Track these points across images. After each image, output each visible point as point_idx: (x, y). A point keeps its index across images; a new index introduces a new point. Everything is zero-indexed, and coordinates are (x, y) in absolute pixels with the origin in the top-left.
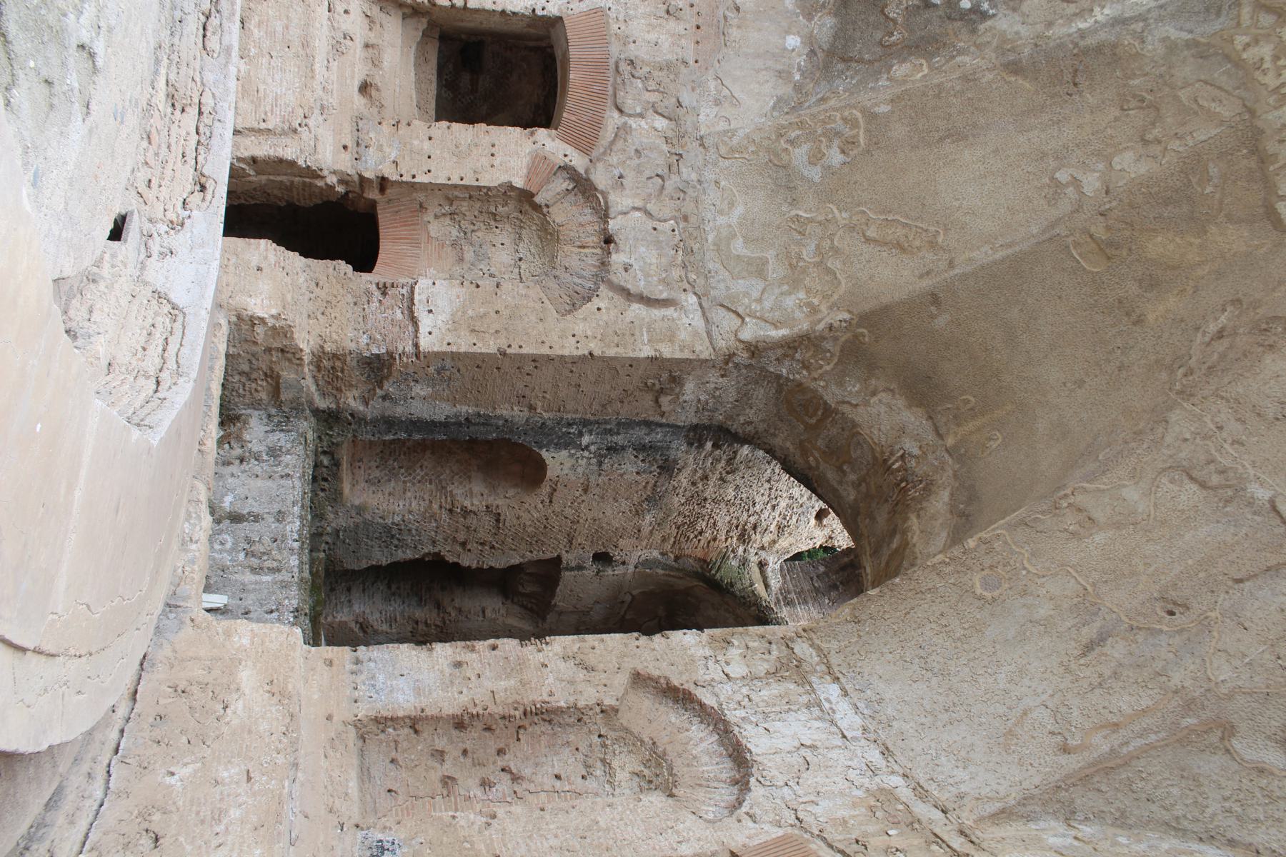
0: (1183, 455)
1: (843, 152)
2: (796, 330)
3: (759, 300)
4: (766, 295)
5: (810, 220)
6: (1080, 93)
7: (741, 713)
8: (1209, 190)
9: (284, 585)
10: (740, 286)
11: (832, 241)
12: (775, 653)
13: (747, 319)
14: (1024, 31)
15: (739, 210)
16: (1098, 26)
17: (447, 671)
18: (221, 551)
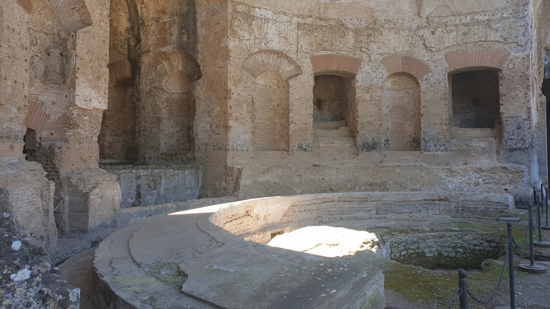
7: (263, 45)
9: (165, 174)
12: (241, 19)
17: (238, 123)
18: (152, 200)
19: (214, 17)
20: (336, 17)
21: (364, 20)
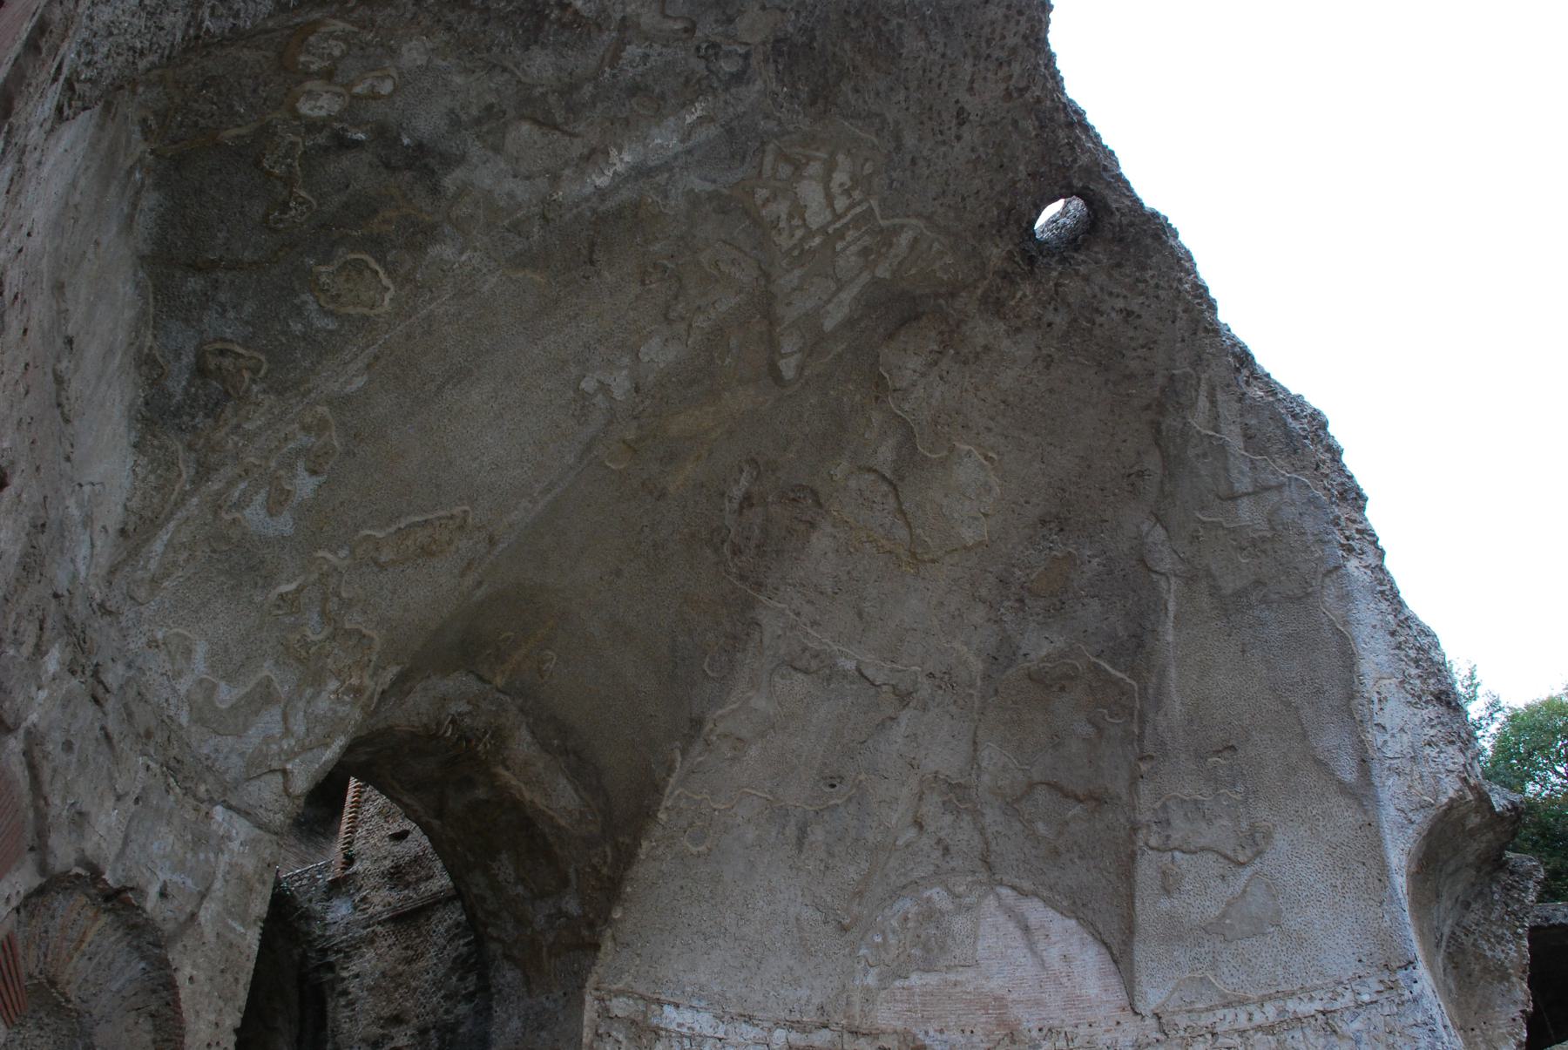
0: (782, 652)
1: (313, 472)
2: (351, 729)
3: (287, 732)
4: (292, 720)
5: (299, 590)
6: (598, 274)
8: (728, 360)
10: (254, 736)
11: (339, 595)
12: (621, 1037)
13: (289, 766)
14: (521, 190)
15: (201, 649)
16: (620, 181)
19: (544, 1034)
20: (899, 1025)
21: (978, 1031)
